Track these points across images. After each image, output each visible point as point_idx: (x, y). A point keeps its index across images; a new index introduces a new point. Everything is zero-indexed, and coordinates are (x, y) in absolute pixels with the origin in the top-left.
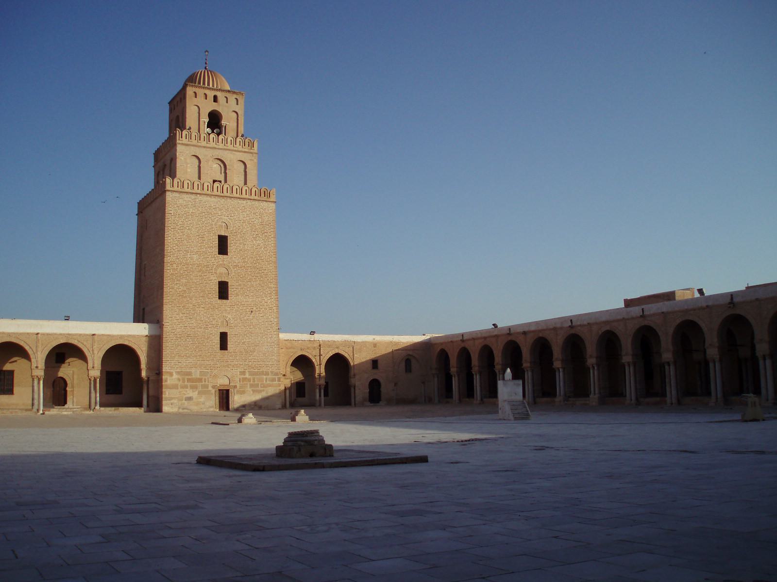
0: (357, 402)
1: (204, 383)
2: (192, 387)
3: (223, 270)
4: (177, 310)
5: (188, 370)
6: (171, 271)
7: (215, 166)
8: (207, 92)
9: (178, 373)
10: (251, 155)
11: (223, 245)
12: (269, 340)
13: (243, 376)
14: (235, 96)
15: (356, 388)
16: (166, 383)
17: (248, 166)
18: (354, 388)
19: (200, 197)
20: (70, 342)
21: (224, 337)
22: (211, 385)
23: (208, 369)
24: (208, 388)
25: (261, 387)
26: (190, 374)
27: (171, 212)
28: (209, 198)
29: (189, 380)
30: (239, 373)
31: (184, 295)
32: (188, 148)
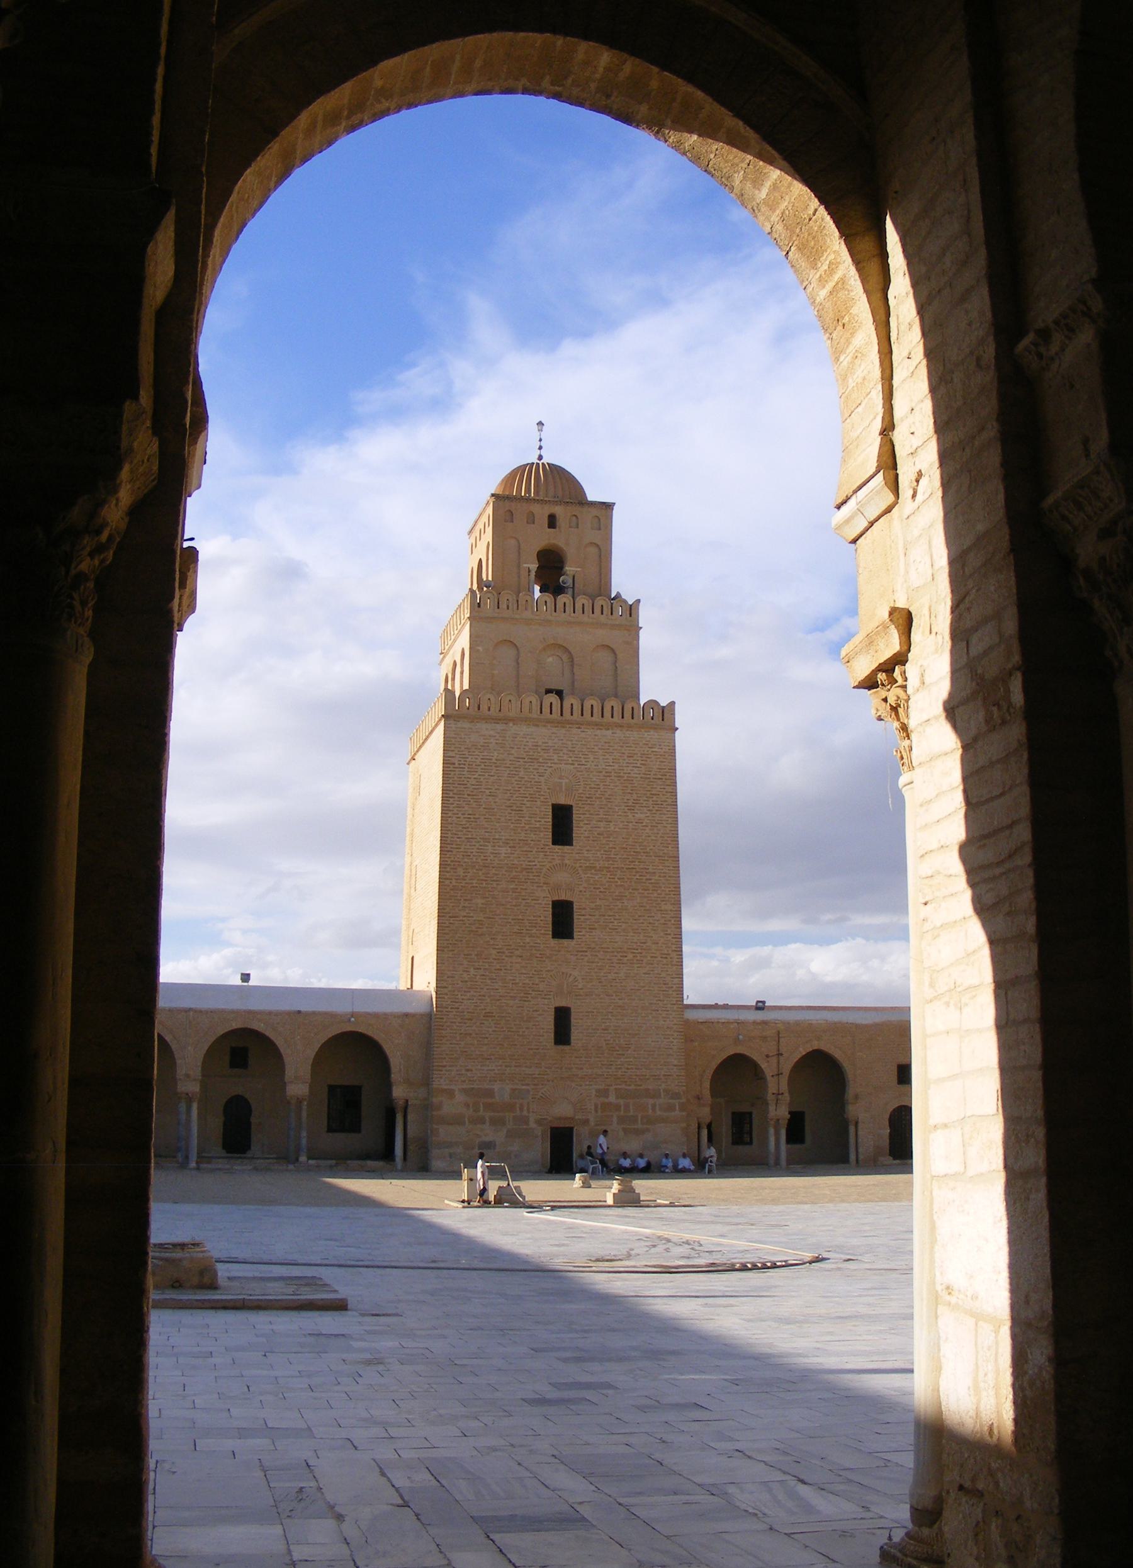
0: (861, 1157)
2: (494, 1122)
3: (562, 877)
4: (465, 962)
6: (454, 881)
7: (550, 659)
8: (536, 509)
11: (562, 825)
13: (603, 1099)
14: (594, 512)
15: (860, 1126)
17: (620, 656)
18: (857, 1123)
21: (562, 1017)
24: (527, 1123)
26: (490, 1093)
27: (453, 760)
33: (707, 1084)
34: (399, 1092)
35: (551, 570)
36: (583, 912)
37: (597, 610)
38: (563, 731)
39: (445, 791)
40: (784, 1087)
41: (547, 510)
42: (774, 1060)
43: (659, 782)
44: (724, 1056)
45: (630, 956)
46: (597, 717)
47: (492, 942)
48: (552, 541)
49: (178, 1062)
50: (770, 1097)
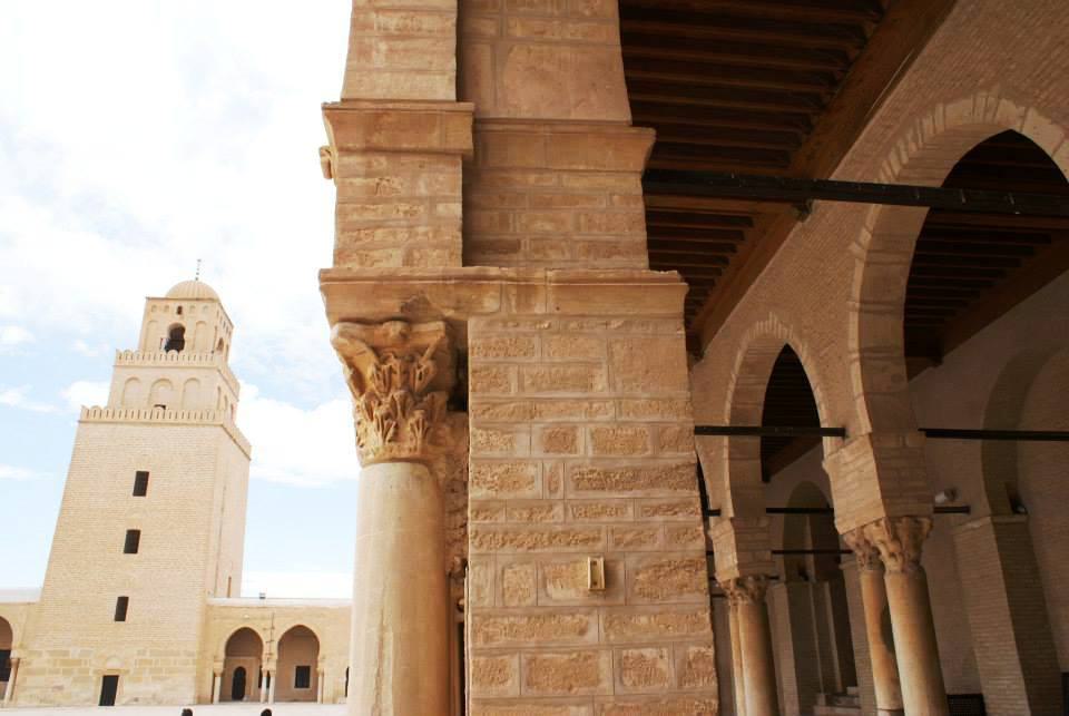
1: (83, 666)
2: (65, 672)
5: (64, 649)
7: (162, 388)
8: (171, 304)
9: (52, 653)
11: (141, 484)
13: (140, 657)
16: (30, 667)
18: (323, 675)
21: (123, 604)
22: (92, 669)
26: (66, 653)
29: (64, 662)
30: (135, 652)
34: (14, 655)
35: (176, 340)
40: (275, 645)
41: (178, 304)
42: (269, 632)
44: (236, 629)
46: (198, 420)
50: (264, 657)
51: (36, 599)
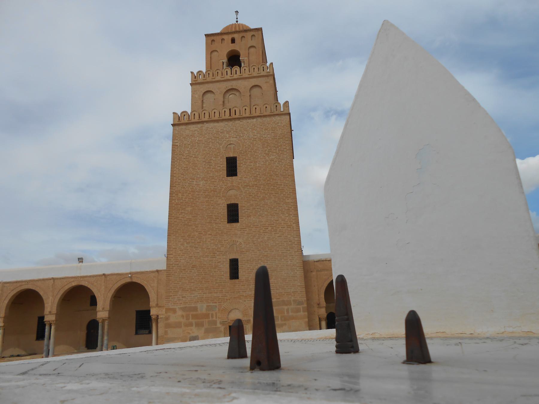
1: (211, 319)
4: (182, 240)
5: (193, 305)
8: (225, 37)
9: (183, 309)
10: (266, 78)
11: (232, 166)
12: (289, 262)
14: (252, 33)
19: (207, 125)
20: (81, 284)
23: (216, 303)
25: (282, 320)
26: (195, 309)
27: (177, 144)
28: (216, 124)
29: (194, 317)
31: (190, 224)
32: (201, 86)
33: (322, 296)
34: (153, 312)
35: (234, 60)
36: (244, 208)
37: (252, 70)
38: (231, 123)
39: (173, 158)
43: (281, 140)
45: (270, 228)
47: (196, 229)
48: (233, 49)
49: (46, 305)
51: (163, 266)
